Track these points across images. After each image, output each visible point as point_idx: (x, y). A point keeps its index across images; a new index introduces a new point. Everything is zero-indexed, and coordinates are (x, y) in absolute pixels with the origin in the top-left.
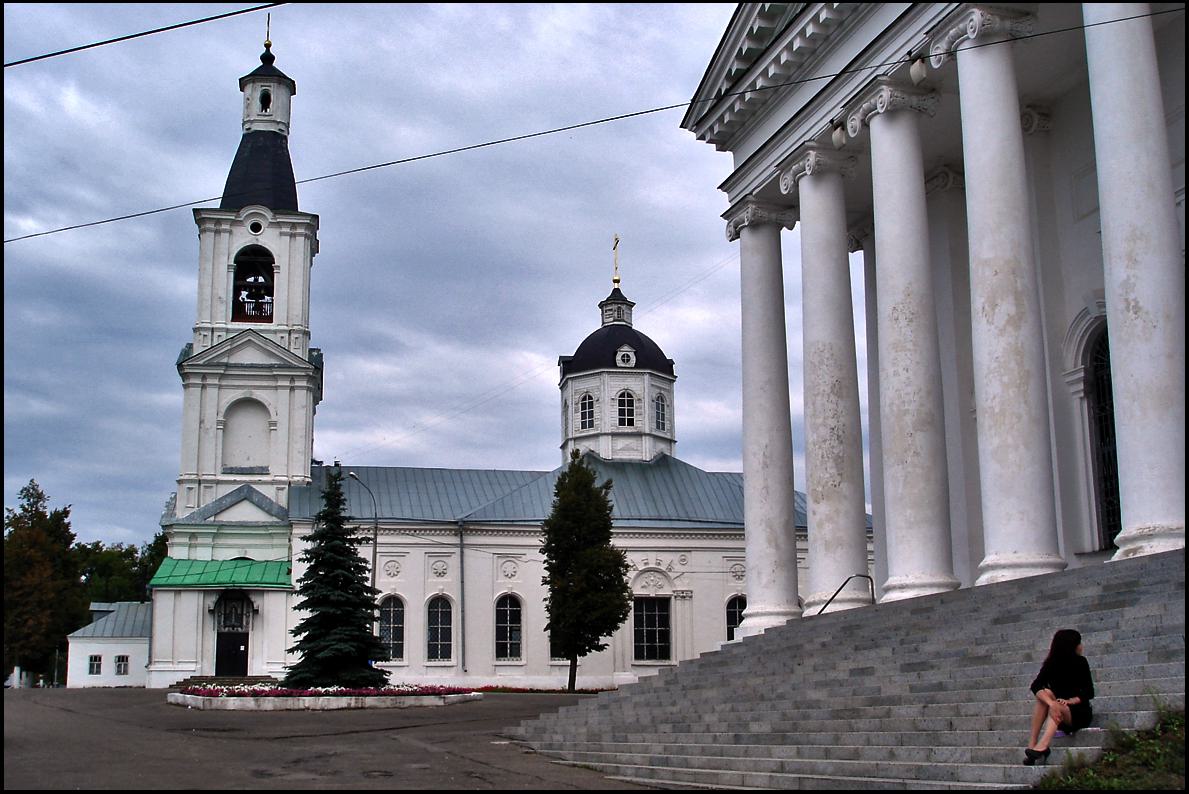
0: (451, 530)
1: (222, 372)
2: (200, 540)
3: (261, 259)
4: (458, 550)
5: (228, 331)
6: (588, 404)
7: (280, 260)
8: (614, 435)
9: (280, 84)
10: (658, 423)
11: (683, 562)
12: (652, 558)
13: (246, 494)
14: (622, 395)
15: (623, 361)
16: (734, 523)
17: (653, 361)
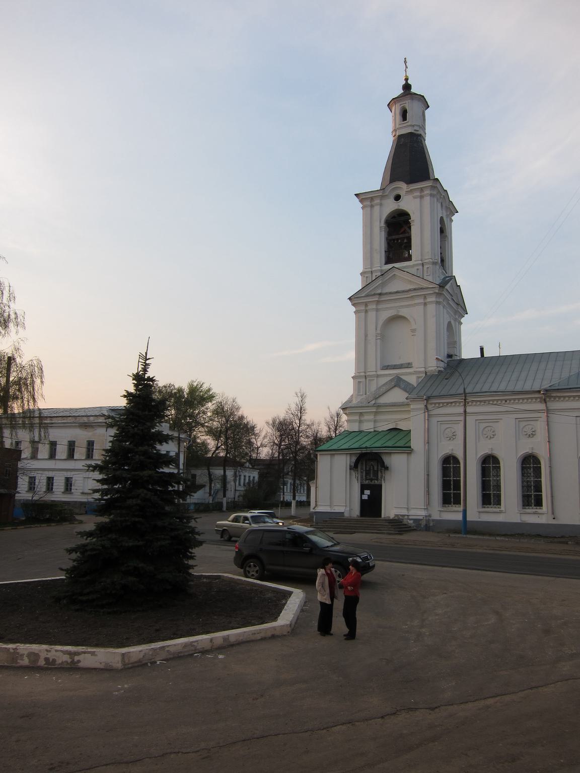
0: (536, 398)
1: (377, 299)
9: (413, 100)
13: (398, 382)
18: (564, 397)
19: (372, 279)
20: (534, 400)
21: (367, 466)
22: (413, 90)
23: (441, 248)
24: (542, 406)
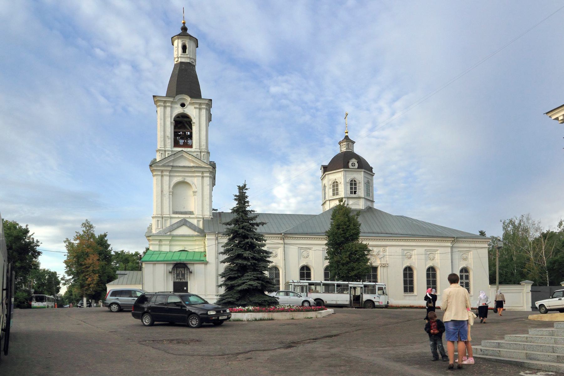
0: (279, 237)
2: (164, 243)
3: (186, 119)
4: (282, 246)
5: (172, 151)
6: (335, 185)
7: (195, 120)
11: (384, 251)
14: (352, 181)
15: (352, 165)
16: (407, 235)
17: (363, 165)
18: (293, 237)
20: (277, 238)
21: (178, 271)
22: (189, 32)
24: (282, 241)
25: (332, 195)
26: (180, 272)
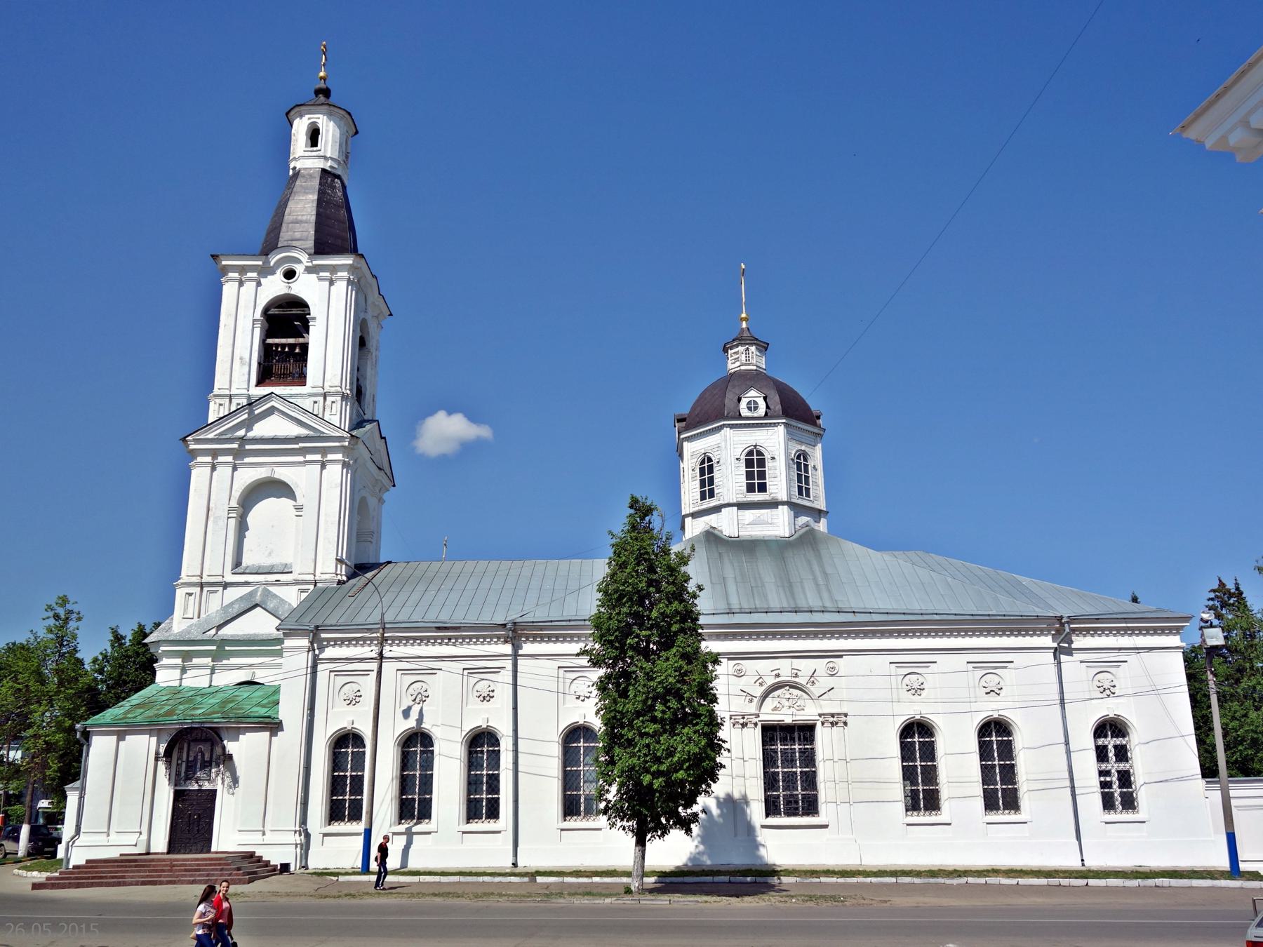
3: (295, 311)
4: (508, 664)
7: (316, 310)
8: (741, 506)
10: (800, 488)
12: (785, 668)
14: (750, 453)
15: (749, 409)
19: (230, 410)
21: (191, 752)
23: (358, 370)
24: (508, 649)
25: (699, 497)
26: (199, 757)
